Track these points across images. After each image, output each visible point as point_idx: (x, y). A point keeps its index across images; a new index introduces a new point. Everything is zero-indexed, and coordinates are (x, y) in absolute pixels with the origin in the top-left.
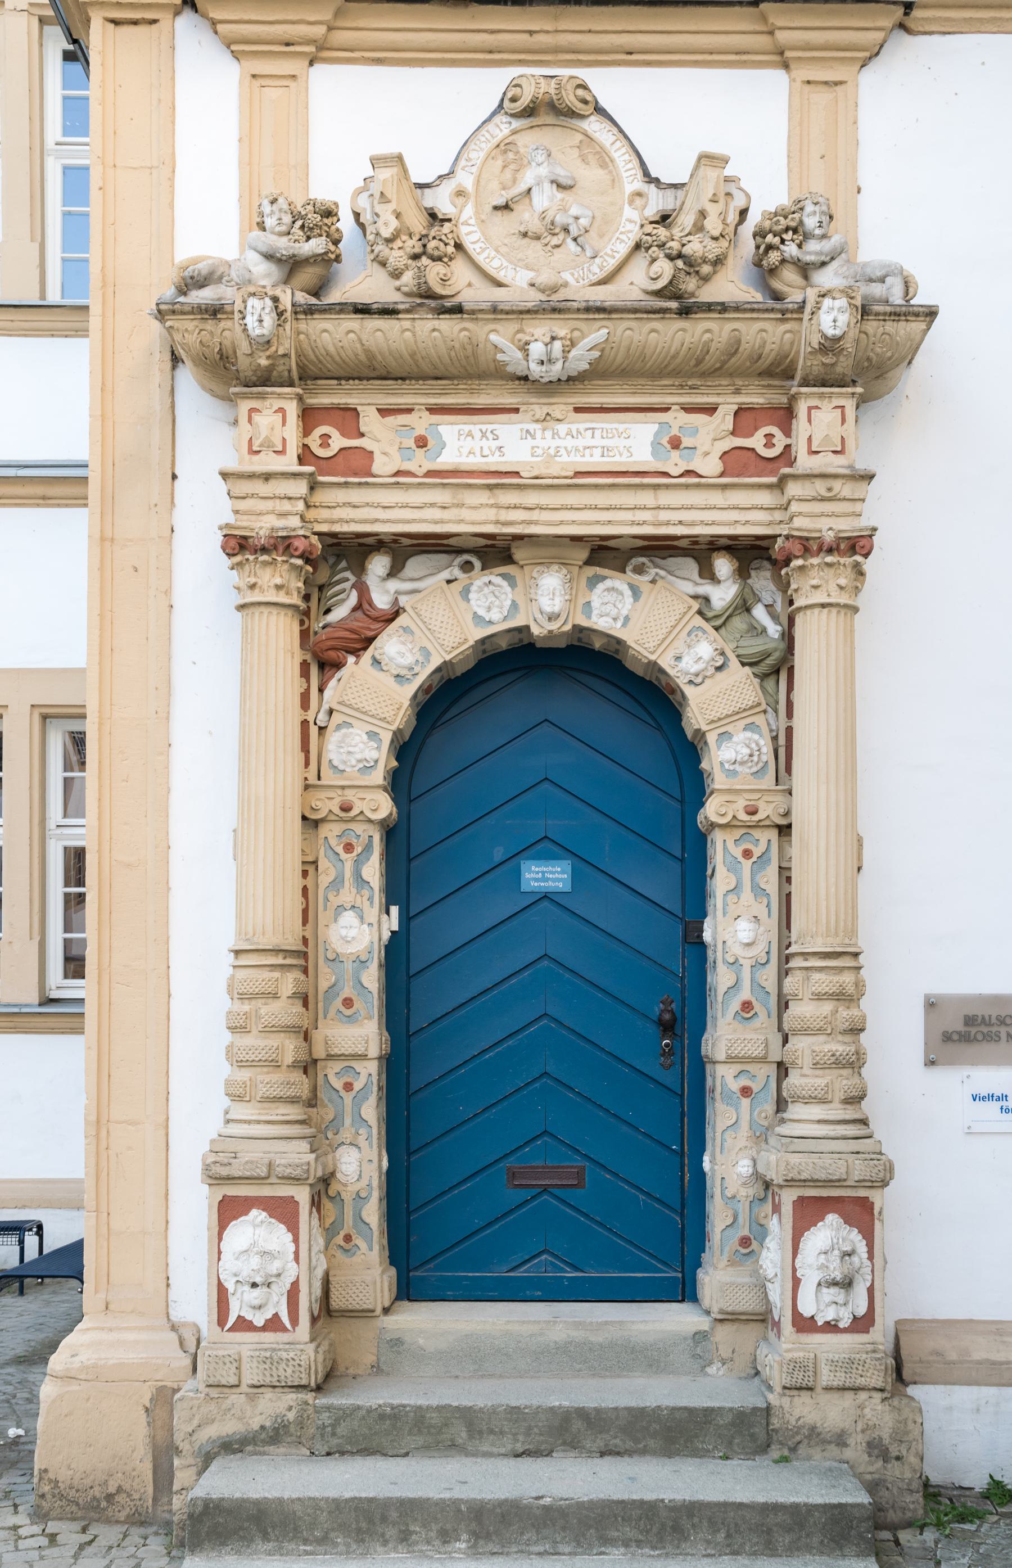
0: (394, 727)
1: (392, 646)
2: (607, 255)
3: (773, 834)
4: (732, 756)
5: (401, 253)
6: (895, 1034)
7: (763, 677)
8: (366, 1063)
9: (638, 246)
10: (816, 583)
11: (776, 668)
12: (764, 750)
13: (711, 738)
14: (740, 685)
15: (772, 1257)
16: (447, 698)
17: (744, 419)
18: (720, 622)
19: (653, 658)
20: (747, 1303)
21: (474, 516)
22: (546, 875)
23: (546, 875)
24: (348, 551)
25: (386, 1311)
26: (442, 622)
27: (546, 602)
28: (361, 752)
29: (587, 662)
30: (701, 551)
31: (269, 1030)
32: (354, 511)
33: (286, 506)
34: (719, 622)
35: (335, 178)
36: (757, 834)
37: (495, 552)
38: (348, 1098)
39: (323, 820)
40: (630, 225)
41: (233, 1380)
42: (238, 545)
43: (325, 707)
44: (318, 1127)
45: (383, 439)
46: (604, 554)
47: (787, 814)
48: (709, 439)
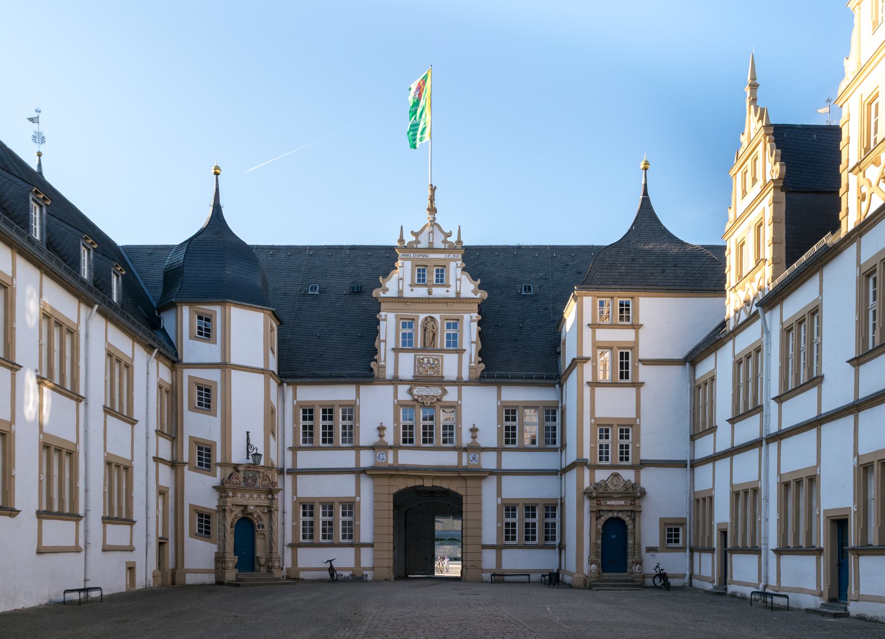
2: (620, 488)
4: (630, 527)
10: (637, 515)
11: (634, 520)
14: (631, 522)
16: (607, 522)
21: (610, 508)
22: (614, 536)
23: (614, 536)
24: (599, 511)
26: (605, 517)
27: (615, 514)
28: (600, 527)
29: (618, 519)
35: (597, 480)
37: (611, 511)
42: (591, 512)
45: (603, 503)
48: (629, 502)
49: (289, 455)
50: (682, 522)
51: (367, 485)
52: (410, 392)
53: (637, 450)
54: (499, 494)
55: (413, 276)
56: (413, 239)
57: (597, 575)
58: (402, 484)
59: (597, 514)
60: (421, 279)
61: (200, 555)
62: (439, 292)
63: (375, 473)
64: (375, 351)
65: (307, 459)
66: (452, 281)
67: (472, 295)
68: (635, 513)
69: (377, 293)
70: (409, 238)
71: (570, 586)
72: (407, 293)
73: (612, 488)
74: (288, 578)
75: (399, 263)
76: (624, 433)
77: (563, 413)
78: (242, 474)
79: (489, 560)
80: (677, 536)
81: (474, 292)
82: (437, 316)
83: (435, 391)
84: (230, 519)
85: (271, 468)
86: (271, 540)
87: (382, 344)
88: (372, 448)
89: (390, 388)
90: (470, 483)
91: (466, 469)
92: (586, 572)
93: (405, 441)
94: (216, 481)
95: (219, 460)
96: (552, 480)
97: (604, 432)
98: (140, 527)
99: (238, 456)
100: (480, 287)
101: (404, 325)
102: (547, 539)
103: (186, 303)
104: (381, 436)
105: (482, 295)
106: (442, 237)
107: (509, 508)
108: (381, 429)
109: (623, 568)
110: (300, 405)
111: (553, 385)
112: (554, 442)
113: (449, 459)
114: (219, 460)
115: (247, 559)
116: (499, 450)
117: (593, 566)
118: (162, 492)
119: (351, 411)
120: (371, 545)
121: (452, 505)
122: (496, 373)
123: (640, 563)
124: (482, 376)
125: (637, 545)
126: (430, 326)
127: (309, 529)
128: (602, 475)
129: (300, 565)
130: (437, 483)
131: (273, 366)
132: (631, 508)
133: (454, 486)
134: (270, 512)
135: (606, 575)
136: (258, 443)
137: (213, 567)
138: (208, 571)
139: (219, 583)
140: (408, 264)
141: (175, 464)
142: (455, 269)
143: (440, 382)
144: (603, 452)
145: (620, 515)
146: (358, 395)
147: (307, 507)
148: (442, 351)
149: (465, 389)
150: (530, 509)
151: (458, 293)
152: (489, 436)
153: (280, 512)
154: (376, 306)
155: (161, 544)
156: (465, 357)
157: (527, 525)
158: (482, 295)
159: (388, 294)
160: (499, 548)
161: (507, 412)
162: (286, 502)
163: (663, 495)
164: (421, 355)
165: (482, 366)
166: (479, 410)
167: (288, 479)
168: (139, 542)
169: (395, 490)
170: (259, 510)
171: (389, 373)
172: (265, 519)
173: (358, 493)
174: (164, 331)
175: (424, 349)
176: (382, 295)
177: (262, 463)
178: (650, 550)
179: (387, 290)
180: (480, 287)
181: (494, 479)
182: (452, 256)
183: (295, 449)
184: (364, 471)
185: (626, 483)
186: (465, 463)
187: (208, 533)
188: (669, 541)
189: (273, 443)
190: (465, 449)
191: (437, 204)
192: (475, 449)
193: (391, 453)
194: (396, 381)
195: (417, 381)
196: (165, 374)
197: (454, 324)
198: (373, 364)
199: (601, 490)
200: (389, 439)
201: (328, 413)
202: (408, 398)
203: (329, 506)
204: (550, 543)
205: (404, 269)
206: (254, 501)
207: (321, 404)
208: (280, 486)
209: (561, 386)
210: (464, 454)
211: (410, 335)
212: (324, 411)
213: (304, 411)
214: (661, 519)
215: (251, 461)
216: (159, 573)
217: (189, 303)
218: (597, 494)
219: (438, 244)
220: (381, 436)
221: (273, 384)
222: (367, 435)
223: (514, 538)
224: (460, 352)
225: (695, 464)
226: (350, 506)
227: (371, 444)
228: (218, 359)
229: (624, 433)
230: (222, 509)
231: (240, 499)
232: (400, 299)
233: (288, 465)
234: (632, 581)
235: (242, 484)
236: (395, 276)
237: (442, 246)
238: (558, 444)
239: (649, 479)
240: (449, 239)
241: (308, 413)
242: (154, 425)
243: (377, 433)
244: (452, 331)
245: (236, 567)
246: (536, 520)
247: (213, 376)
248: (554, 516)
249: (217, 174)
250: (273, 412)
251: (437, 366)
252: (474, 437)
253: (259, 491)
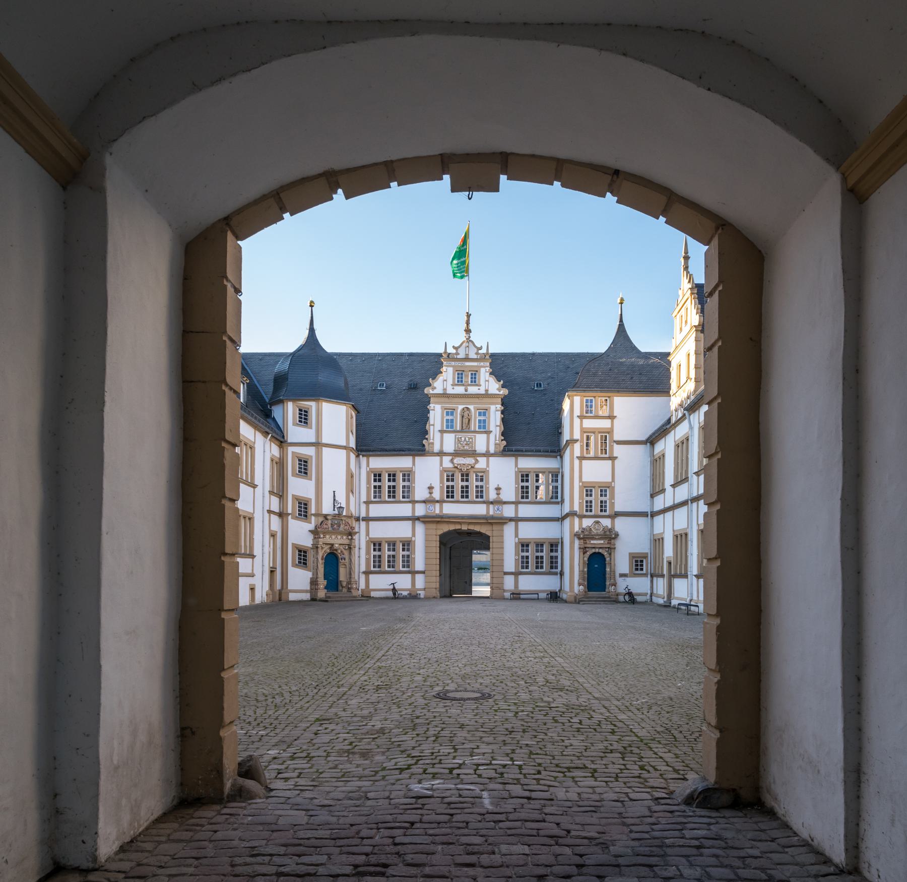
2: (600, 531)
4: (608, 559)
6: (617, 575)
11: (610, 554)
16: (591, 555)
27: (597, 550)
28: (586, 559)
29: (599, 553)
35: (584, 526)
44: (584, 580)
49: (363, 507)
50: (645, 556)
51: (420, 528)
52: (452, 461)
53: (613, 504)
54: (517, 535)
55: (454, 379)
56: (454, 351)
58: (446, 528)
59: (584, 550)
60: (460, 381)
61: (299, 580)
62: (473, 390)
63: (426, 520)
64: (426, 432)
65: (376, 510)
66: (482, 382)
67: (498, 392)
68: (611, 549)
69: (428, 391)
70: (451, 350)
71: (566, 602)
72: (450, 391)
74: (362, 596)
75: (444, 369)
76: (603, 493)
77: (562, 476)
78: (330, 522)
79: (509, 583)
80: (642, 565)
81: (499, 390)
82: (471, 407)
83: (470, 461)
84: (321, 553)
85: (351, 517)
86: (350, 568)
87: (432, 427)
88: (424, 502)
89: (438, 458)
90: (495, 527)
91: (492, 517)
92: (576, 591)
93: (448, 497)
94: (312, 526)
95: (313, 512)
96: (556, 525)
97: (589, 493)
98: (258, 560)
99: (327, 508)
100: (503, 386)
101: (447, 414)
102: (552, 568)
103: (290, 400)
104: (431, 493)
105: (505, 392)
106: (475, 350)
107: (524, 545)
108: (431, 488)
109: (603, 588)
110: (371, 470)
111: (556, 457)
112: (557, 497)
113: (479, 510)
114: (313, 512)
115: (333, 583)
116: (516, 503)
117: (581, 587)
118: (273, 535)
119: (408, 475)
120: (423, 572)
121: (483, 542)
122: (514, 448)
123: (615, 585)
124: (504, 450)
125: (613, 572)
126: (466, 414)
127: (378, 560)
128: (587, 523)
129: (371, 587)
130: (471, 527)
131: (353, 444)
133: (484, 530)
134: (350, 548)
135: (591, 593)
136: (342, 500)
137: (309, 588)
138: (306, 591)
139: (313, 599)
140: (450, 370)
141: (282, 515)
142: (484, 373)
143: (474, 454)
144: (589, 505)
145: (601, 551)
146: (414, 464)
147: (377, 545)
148: (475, 432)
149: (491, 458)
150: (539, 545)
151: (487, 391)
152: (510, 493)
153: (357, 549)
154: (427, 400)
155: (272, 572)
156: (492, 436)
157: (537, 558)
158: (505, 392)
159: (435, 392)
160: (516, 574)
161: (522, 476)
162: (361, 541)
163: (631, 538)
164: (459, 435)
165: (504, 443)
166: (502, 474)
167: (363, 524)
168: (258, 571)
169: (440, 532)
170: (341, 547)
171: (437, 448)
172: (346, 553)
173: (414, 535)
174: (274, 419)
175: (462, 431)
176: (431, 392)
177: (344, 514)
178: (622, 575)
179: (434, 388)
180: (503, 386)
181: (512, 525)
182: (482, 364)
183: (368, 503)
184: (418, 519)
185: (605, 529)
186: (491, 513)
187: (305, 564)
188: (637, 569)
189: (352, 499)
190: (492, 503)
191: (471, 327)
192: (499, 502)
193: (438, 505)
194: (441, 454)
195: (456, 454)
196: (275, 451)
197: (484, 412)
198: (424, 442)
199: (587, 533)
200: (437, 495)
201: (392, 476)
202: (451, 465)
203: (392, 544)
204: (554, 570)
205: (448, 373)
206: (338, 541)
207: (387, 470)
208: (357, 530)
209: (561, 457)
210: (491, 506)
211: (452, 420)
212: (389, 475)
213: (375, 475)
215: (336, 512)
216: (270, 592)
217: (293, 400)
218: (584, 536)
219: (472, 355)
220: (431, 493)
221: (353, 456)
222: (420, 493)
223: (527, 567)
224: (488, 433)
225: (653, 514)
226: (407, 544)
227: (423, 499)
228: (313, 440)
229: (603, 493)
230: (316, 547)
231: (329, 539)
232: (445, 395)
233: (363, 514)
234: (609, 597)
235: (330, 529)
236: (440, 378)
237: (475, 357)
238: (559, 499)
239: (621, 525)
240: (480, 352)
241: (378, 476)
242: (268, 488)
243: (428, 491)
244: (482, 418)
245: (325, 588)
246: (544, 554)
247: (310, 451)
248: (556, 551)
249: (311, 306)
250: (352, 476)
251: (471, 443)
252: (498, 494)
253: (341, 533)
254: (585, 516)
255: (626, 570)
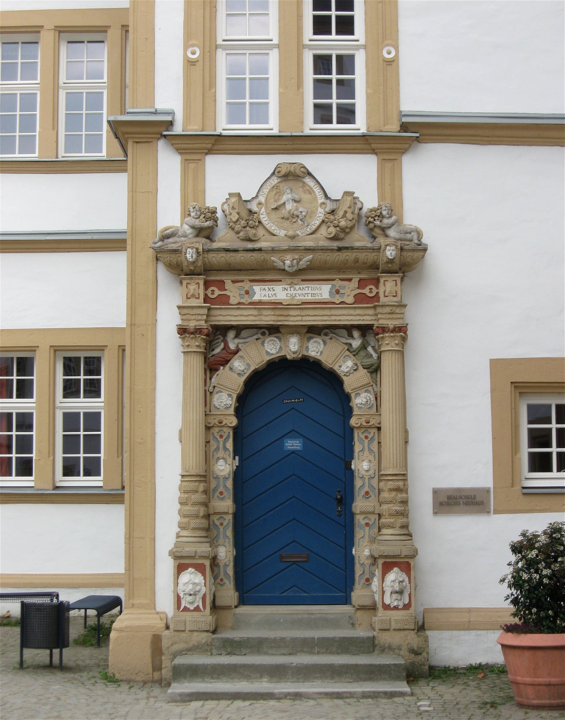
0: (237, 393)
1: (237, 364)
3: (375, 430)
4: (359, 401)
5: (239, 226)
7: (371, 373)
8: (228, 515)
9: (323, 221)
11: (375, 370)
12: (372, 399)
13: (353, 395)
14: (363, 376)
15: (375, 583)
16: (256, 381)
17: (362, 283)
18: (355, 353)
19: (331, 366)
20: (367, 602)
23: (293, 444)
25: (236, 607)
27: (293, 347)
28: (225, 401)
29: (308, 367)
30: (349, 329)
31: (194, 504)
32: (225, 317)
33: (200, 317)
34: (354, 353)
35: (215, 197)
36: (370, 430)
37: (273, 330)
38: (221, 528)
39: (213, 427)
40: (320, 214)
41: (183, 629)
43: (212, 385)
45: (233, 292)
46: (313, 331)
47: (380, 423)
48: (350, 290)
53: (387, 72)
57: (206, 618)
59: (211, 343)
68: (379, 336)
73: (275, 231)
92: (165, 604)
109: (335, 581)
123: (405, 563)
125: (401, 482)
128: (233, 179)
132: (362, 316)
135: (259, 620)
145: (316, 349)
178: (454, 501)
185: (348, 219)
214: (498, 366)
218: (210, 261)
234: (370, 645)
239: (436, 194)
254: (220, 144)
255: (476, 470)
